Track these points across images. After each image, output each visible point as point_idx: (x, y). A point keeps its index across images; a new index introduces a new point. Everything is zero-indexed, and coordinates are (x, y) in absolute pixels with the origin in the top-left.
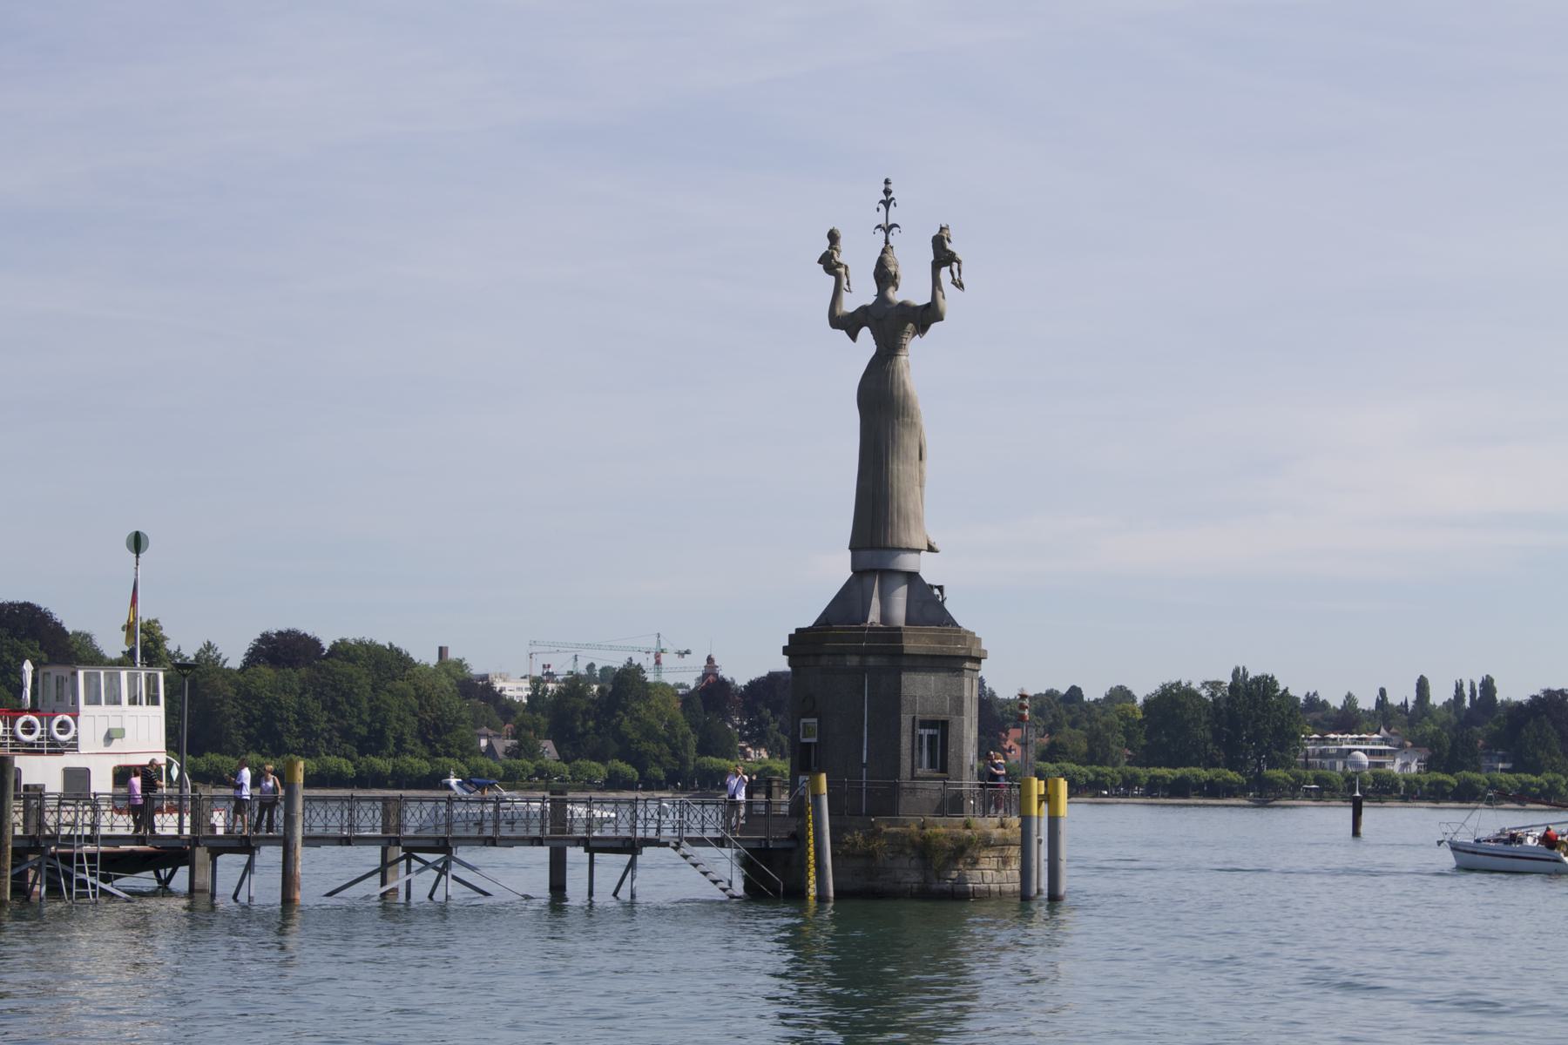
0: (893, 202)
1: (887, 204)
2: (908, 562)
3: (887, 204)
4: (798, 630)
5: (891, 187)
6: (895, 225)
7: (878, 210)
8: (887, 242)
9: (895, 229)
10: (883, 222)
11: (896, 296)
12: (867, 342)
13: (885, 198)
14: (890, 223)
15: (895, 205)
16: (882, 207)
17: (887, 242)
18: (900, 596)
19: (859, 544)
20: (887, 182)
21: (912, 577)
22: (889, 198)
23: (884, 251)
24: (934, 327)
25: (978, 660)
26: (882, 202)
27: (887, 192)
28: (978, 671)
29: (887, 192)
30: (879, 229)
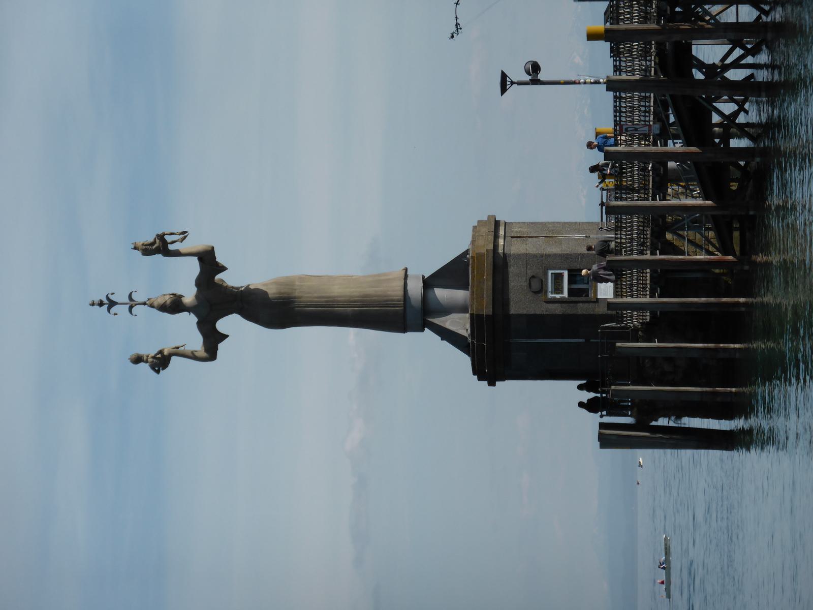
0: (111, 297)
1: (112, 304)
2: (415, 289)
3: (112, 304)
4: (474, 374)
5: (97, 300)
6: (130, 296)
7: (116, 314)
8: (145, 304)
9: (134, 297)
10: (128, 306)
11: (189, 294)
12: (229, 324)
13: (106, 307)
14: (127, 300)
15: (113, 294)
16: (114, 309)
17: (145, 304)
18: (442, 294)
19: (402, 326)
20: (93, 304)
21: (429, 283)
22: (105, 301)
23: (152, 306)
24: (220, 258)
25: (497, 223)
26: (109, 310)
27: (101, 304)
28: (505, 223)
29: (101, 304)
30: (134, 309)
